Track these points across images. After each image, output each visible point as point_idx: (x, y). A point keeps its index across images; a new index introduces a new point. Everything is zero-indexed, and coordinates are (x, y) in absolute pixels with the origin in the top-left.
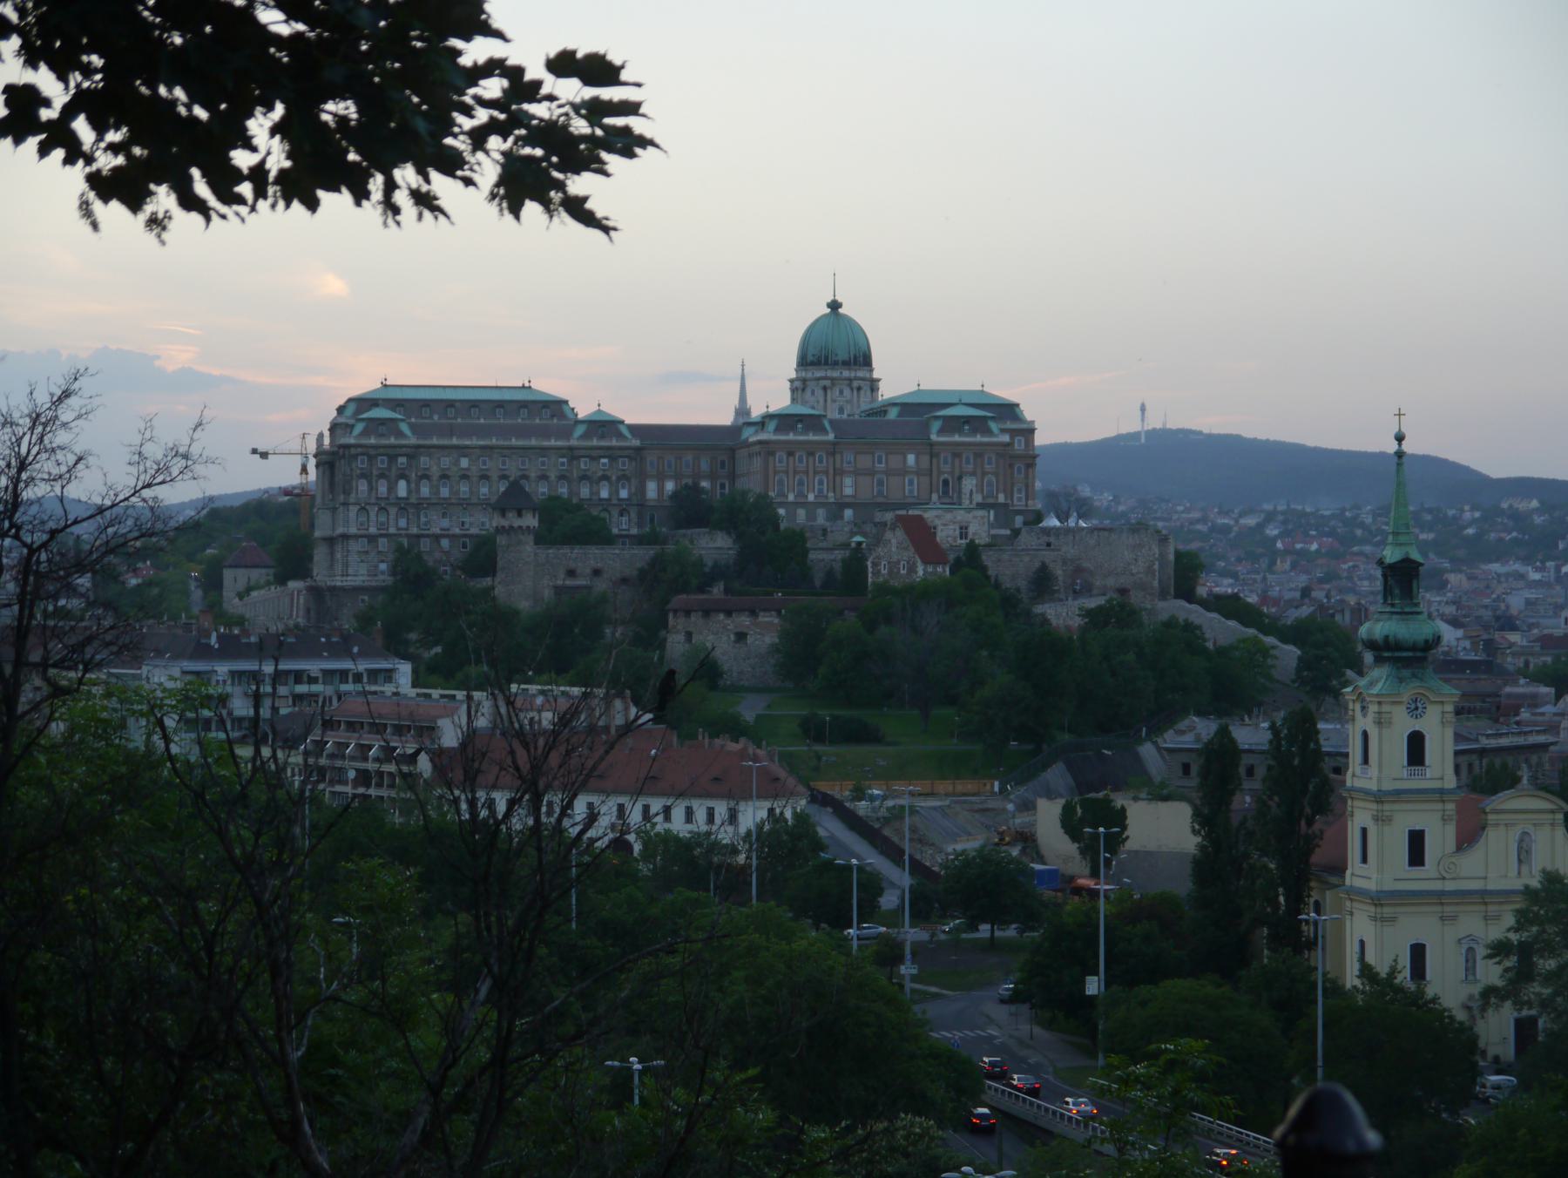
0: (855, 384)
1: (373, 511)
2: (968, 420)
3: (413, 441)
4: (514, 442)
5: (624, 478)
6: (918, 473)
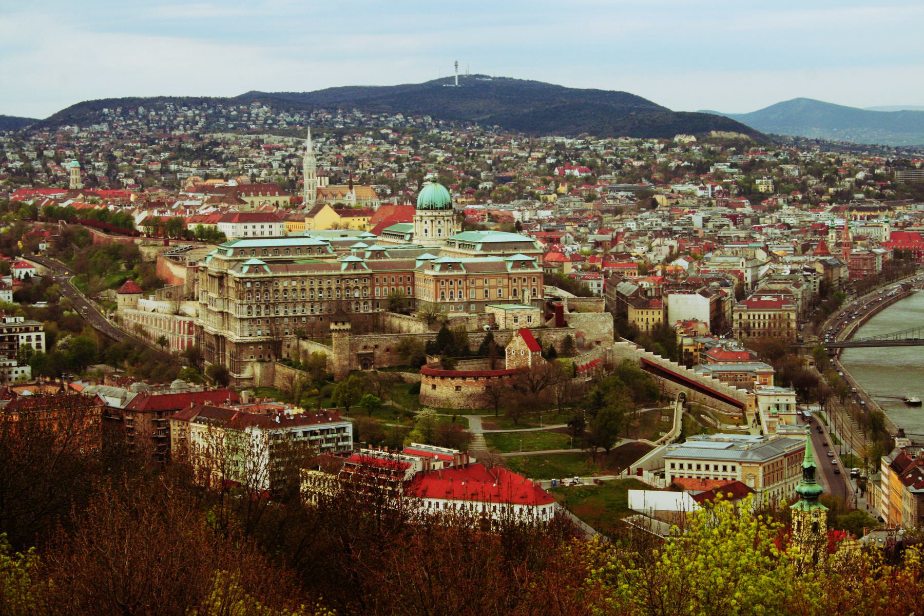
0: (446, 218)
1: (254, 307)
3: (270, 274)
4: (316, 273)
5: (365, 288)
6: (503, 287)
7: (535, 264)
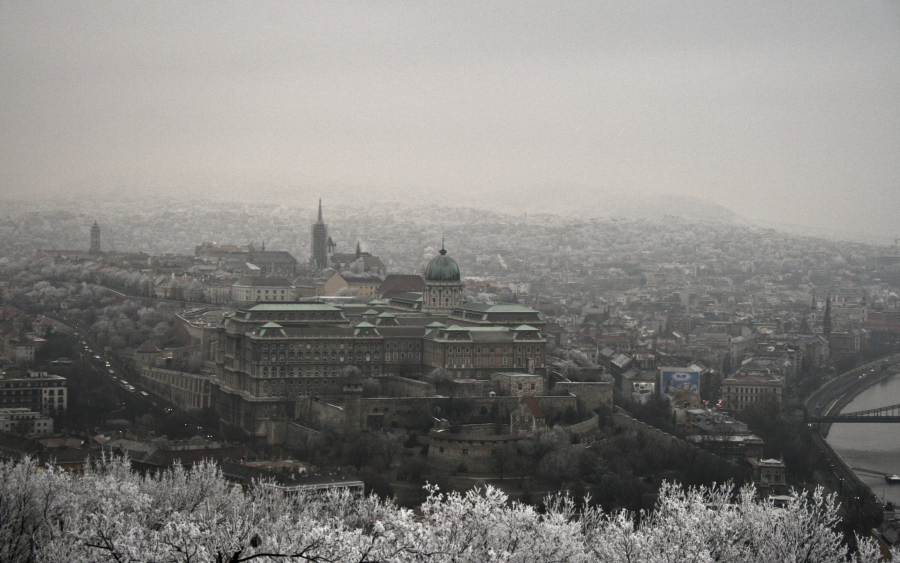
2: (529, 332)
4: (330, 337)
5: (376, 352)
6: (508, 355)
7: (539, 334)
